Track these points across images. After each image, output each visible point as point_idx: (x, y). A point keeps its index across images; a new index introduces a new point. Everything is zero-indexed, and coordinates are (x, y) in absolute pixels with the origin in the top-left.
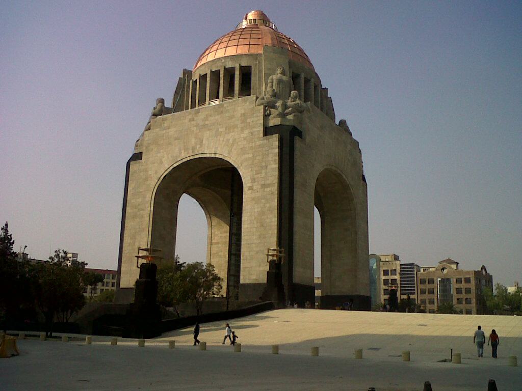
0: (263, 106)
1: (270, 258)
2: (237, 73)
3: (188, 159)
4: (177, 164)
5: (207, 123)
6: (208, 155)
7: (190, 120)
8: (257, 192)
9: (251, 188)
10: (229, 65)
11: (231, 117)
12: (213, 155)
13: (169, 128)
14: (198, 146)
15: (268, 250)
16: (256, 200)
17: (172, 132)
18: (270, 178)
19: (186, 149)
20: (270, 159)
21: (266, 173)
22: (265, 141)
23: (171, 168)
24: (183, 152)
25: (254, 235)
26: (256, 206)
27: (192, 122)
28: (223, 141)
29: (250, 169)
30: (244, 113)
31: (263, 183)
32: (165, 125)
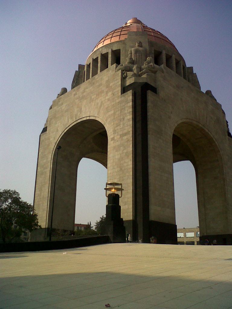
0: (120, 71)
1: (109, 192)
2: (110, 56)
3: (73, 124)
4: (67, 129)
5: (85, 94)
6: (85, 119)
7: (75, 95)
8: (117, 141)
9: (113, 139)
10: (104, 52)
11: (100, 85)
12: (88, 118)
13: (62, 104)
14: (79, 113)
15: (107, 184)
16: (117, 149)
17: (64, 107)
18: (126, 128)
19: (72, 118)
20: (126, 112)
21: (124, 124)
22: (123, 98)
23: (63, 134)
24: (70, 120)
25: (115, 179)
26: (116, 153)
27: (77, 96)
28: (95, 105)
29: (112, 123)
30: (108, 80)
31: (121, 133)
32: (60, 102)
